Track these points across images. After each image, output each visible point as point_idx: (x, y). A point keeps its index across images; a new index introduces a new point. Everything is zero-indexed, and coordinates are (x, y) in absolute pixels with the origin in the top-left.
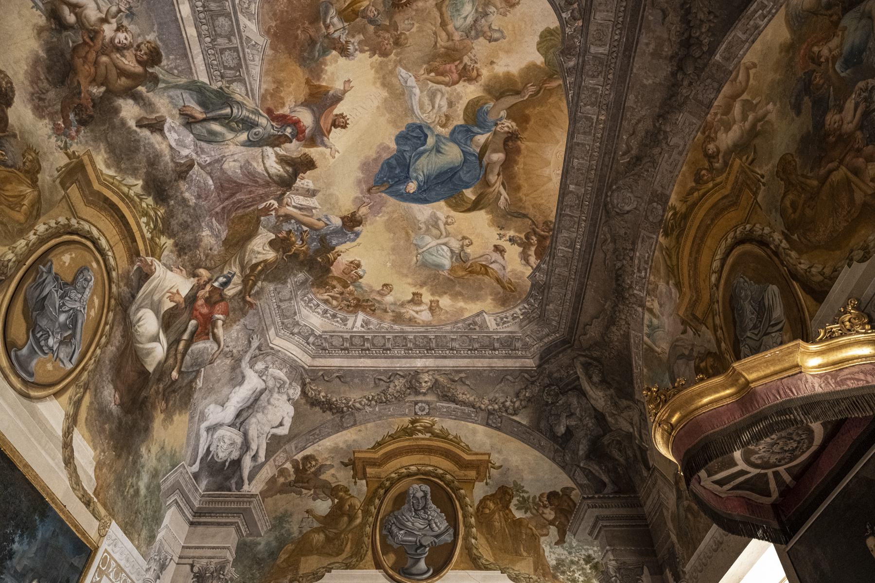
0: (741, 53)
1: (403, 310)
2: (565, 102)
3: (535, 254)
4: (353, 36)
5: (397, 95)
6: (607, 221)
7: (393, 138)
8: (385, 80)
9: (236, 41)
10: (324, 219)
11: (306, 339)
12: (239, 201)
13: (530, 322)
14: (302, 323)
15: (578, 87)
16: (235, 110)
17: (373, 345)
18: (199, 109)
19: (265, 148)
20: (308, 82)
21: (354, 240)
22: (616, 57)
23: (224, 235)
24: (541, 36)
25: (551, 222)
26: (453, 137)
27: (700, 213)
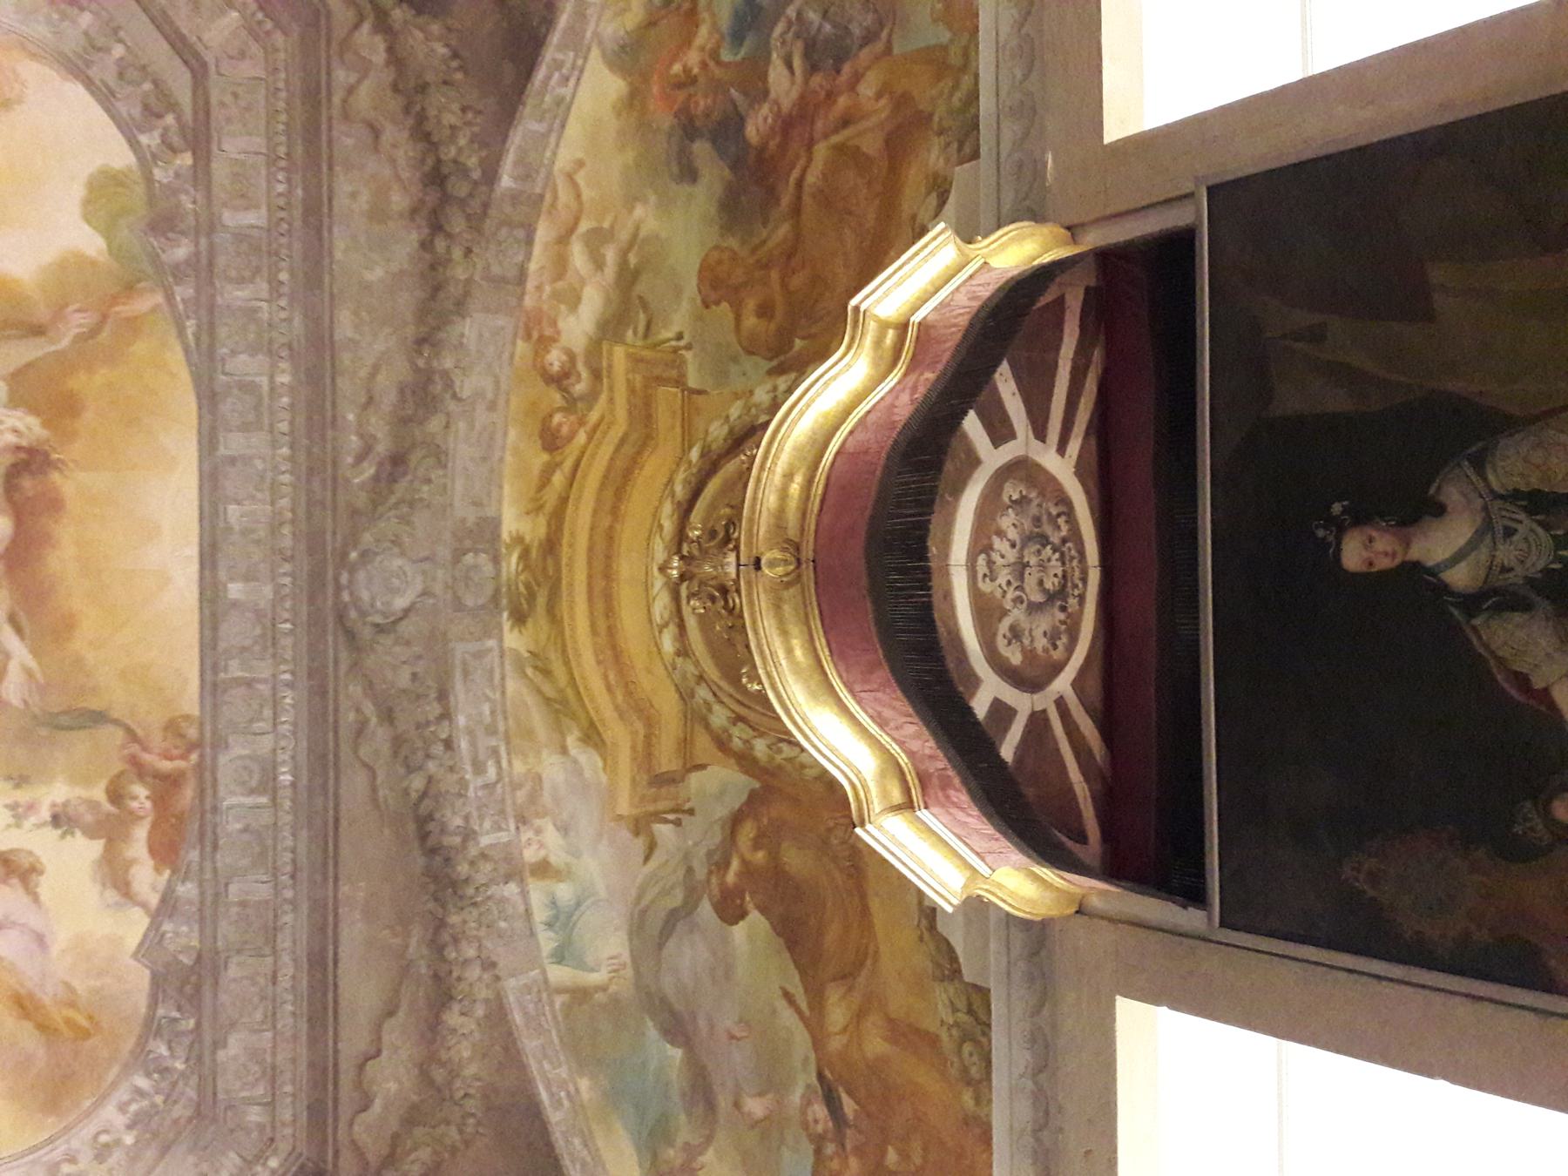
0: (548, 154)
2: (178, 349)
3: (152, 851)
6: (355, 665)
13: (165, 1149)
15: (209, 312)
25: (187, 717)
27: (581, 517)
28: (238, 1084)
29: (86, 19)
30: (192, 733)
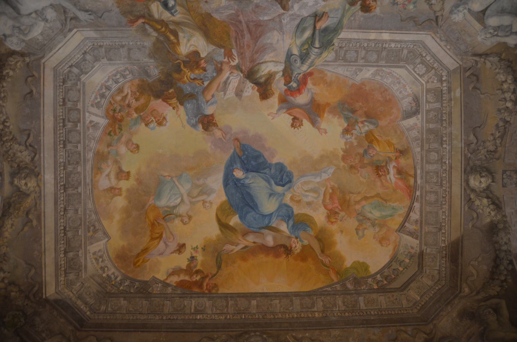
1: (110, 162)
2: (322, 286)
4: (356, 139)
5: (315, 165)
7: (281, 161)
8: (326, 158)
9: (361, 62)
10: (213, 100)
11: (77, 65)
12: (243, 36)
13: (99, 284)
14: (97, 65)
16: (316, 50)
17: (70, 131)
18: (324, 26)
19: (284, 65)
20: (328, 104)
21: (188, 122)
22: (360, 315)
23: (216, 16)
24: (363, 263)
25: (218, 290)
26: (283, 206)
28: (112, 304)
29: (407, 261)
30: (214, 291)
